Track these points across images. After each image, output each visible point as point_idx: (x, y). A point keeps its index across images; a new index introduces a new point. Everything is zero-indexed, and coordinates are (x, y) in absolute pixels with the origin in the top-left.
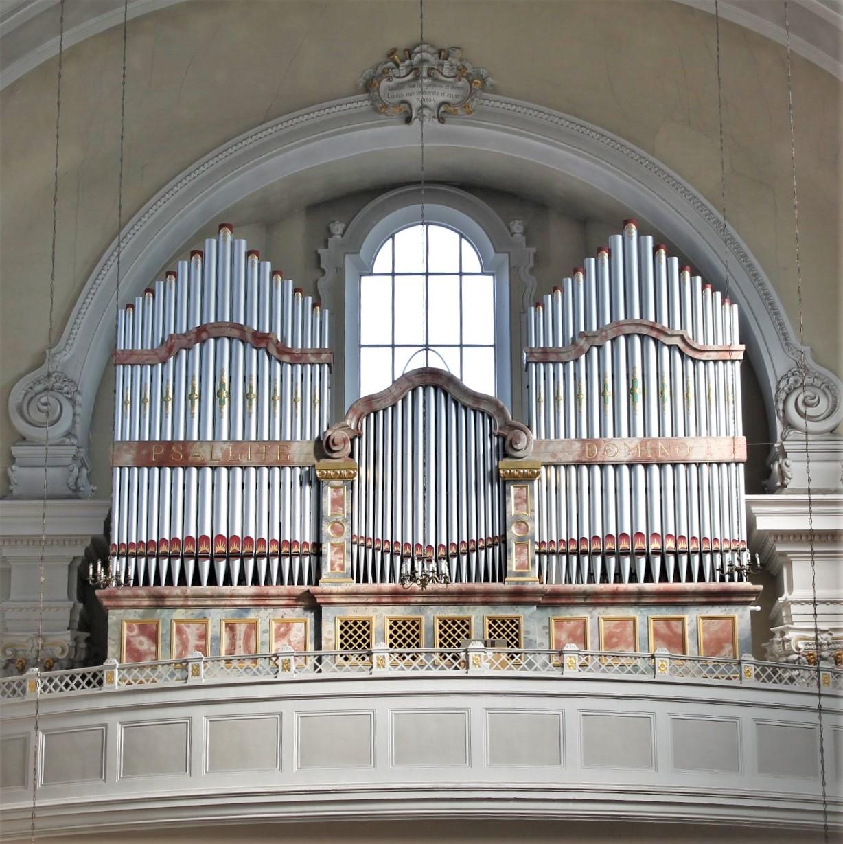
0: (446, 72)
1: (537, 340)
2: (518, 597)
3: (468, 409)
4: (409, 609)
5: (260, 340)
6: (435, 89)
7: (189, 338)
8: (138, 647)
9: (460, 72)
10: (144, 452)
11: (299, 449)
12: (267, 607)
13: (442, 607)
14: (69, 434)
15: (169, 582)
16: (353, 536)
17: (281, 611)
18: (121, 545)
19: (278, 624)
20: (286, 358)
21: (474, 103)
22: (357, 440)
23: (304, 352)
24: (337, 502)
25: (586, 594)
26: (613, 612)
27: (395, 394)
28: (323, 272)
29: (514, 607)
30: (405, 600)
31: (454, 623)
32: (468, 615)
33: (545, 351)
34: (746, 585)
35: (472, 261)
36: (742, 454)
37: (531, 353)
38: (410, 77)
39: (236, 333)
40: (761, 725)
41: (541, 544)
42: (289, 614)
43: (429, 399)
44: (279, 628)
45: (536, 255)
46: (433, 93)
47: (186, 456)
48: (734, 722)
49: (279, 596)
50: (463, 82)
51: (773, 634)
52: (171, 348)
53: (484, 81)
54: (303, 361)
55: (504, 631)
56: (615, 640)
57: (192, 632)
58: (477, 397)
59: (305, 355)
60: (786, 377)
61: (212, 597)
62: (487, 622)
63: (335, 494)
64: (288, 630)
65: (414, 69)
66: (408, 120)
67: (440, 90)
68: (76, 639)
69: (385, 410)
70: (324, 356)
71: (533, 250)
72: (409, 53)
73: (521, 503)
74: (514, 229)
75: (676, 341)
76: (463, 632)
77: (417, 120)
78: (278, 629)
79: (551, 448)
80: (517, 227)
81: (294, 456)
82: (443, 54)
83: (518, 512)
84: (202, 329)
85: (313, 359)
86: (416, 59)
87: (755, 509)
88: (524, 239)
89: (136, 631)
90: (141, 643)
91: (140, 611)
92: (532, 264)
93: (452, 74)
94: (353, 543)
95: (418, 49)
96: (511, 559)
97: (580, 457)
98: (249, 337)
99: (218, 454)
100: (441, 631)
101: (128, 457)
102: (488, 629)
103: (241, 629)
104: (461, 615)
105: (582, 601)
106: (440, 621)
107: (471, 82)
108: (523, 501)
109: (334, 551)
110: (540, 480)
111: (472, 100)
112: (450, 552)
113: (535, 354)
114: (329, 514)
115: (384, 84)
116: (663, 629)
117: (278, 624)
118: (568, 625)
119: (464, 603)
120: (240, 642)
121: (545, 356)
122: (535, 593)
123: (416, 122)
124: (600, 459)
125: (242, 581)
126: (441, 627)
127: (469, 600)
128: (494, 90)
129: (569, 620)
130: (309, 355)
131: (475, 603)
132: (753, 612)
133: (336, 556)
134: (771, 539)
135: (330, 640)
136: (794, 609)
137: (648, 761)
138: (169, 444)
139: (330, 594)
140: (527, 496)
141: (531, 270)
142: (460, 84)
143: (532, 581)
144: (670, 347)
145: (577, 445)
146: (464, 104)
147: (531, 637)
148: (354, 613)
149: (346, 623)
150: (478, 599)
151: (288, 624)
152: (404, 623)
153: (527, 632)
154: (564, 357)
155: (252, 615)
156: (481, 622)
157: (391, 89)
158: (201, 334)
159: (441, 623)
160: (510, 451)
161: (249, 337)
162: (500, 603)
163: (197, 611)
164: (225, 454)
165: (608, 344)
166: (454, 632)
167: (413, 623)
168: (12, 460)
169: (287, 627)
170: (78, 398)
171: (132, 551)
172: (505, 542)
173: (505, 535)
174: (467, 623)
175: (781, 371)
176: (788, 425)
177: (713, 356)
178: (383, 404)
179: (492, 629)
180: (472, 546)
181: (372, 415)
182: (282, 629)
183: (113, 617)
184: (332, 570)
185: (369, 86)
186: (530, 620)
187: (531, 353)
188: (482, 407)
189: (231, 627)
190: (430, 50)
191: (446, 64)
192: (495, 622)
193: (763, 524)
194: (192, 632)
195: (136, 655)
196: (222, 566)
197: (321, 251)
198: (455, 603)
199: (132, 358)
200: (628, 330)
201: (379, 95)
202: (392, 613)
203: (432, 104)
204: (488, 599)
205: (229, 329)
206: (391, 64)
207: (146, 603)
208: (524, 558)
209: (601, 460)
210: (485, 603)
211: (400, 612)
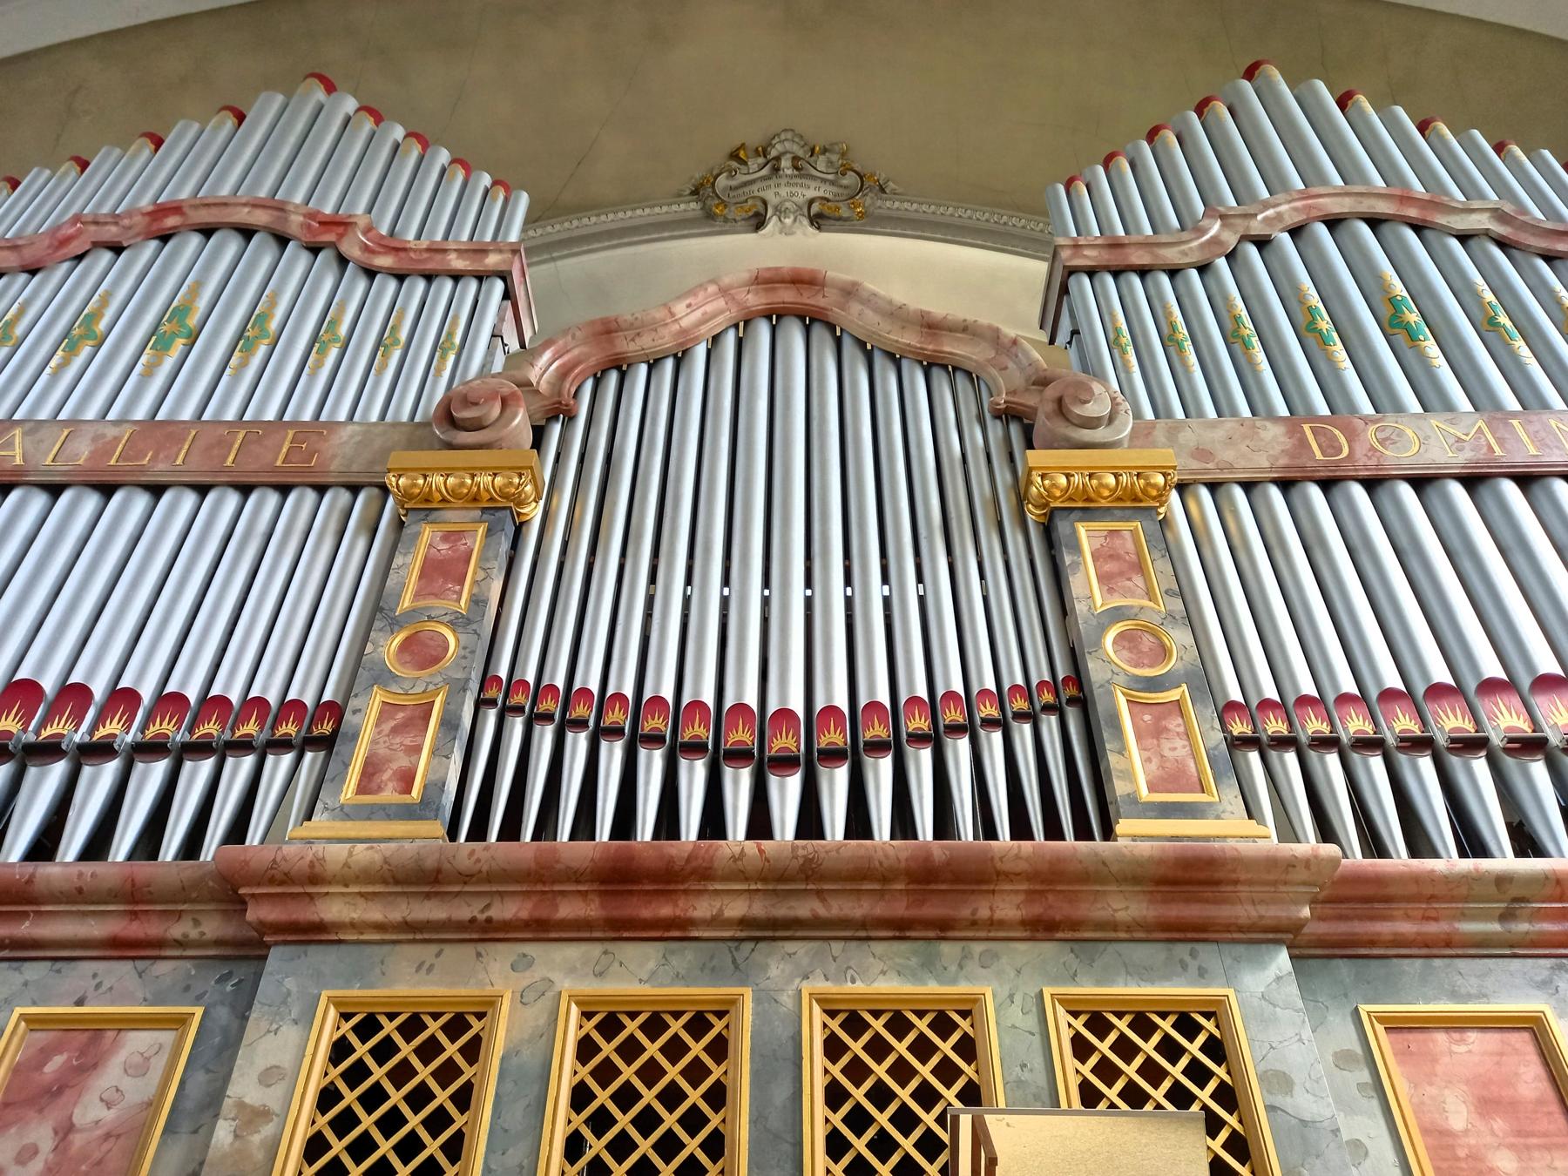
0: (821, 165)
3: (905, 364)
4: (686, 956)
6: (804, 181)
7: (126, 222)
11: (358, 438)
13: (837, 947)
16: (487, 679)
19: (42, 1038)
21: (868, 201)
22: (556, 429)
27: (685, 323)
29: (1182, 950)
30: (665, 911)
31: (899, 1025)
32: (963, 988)
38: (765, 172)
44: (45, 1054)
49: (78, 897)
54: (430, 266)
55: (1153, 1073)
59: (438, 257)
62: (1064, 1027)
63: (444, 546)
64: (87, 1064)
67: (813, 184)
69: (654, 365)
73: (1121, 574)
76: (947, 1072)
77: (774, 218)
81: (334, 456)
83: (1118, 601)
85: (458, 263)
93: (831, 170)
94: (480, 704)
95: (777, 140)
96: (1122, 750)
97: (1293, 457)
99: (82, 452)
100: (836, 1070)
102: (1072, 1062)
104: (932, 988)
106: (832, 1014)
107: (861, 178)
109: (387, 727)
111: (866, 195)
112: (867, 735)
113: (1087, 252)
114: (406, 602)
117: (42, 1038)
118: (1462, 1049)
119: (943, 929)
124: (1365, 464)
126: (833, 1048)
127: (965, 913)
129: (1457, 1025)
130: (453, 256)
131: (993, 929)
133: (398, 740)
135: (263, 1114)
139: (314, 878)
140: (1139, 553)
142: (845, 182)
144: (1464, 238)
145: (1273, 433)
147: (1303, 1103)
149: (367, 1027)
152: (654, 1026)
153: (1280, 1081)
154: (1172, 256)
156: (1031, 1022)
159: (835, 1025)
162: (1110, 932)
166: (902, 1072)
167: (698, 1026)
169: (82, 1053)
172: (1083, 703)
173: (1078, 676)
174: (964, 1024)
179: (1093, 1060)
181: (613, 377)
182: (56, 1062)
184: (362, 789)
190: (797, 140)
191: (822, 158)
192: (1099, 1025)
198: (900, 929)
201: (714, 191)
202: (600, 975)
203: (800, 200)
205: (246, 210)
208: (1176, 748)
209: (1373, 462)
210: (1041, 928)
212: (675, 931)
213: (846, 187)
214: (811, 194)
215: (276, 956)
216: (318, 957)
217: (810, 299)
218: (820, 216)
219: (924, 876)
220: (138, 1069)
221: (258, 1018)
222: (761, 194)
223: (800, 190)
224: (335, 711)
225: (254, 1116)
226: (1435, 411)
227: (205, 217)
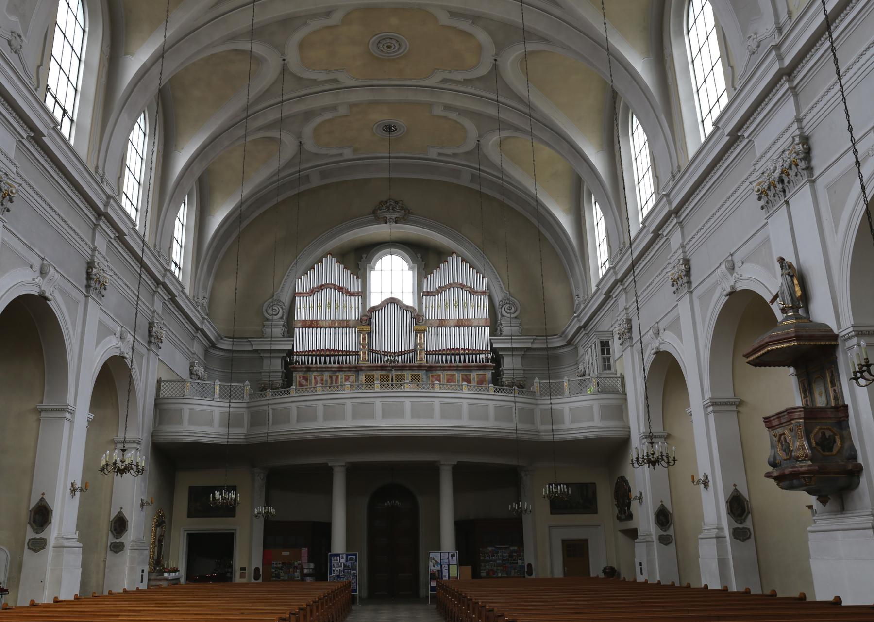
1: (426, 288)
2: (420, 367)
4: (386, 372)
5: (340, 289)
6: (394, 213)
8: (303, 383)
9: (402, 208)
10: (304, 323)
12: (342, 371)
14: (281, 318)
15: (312, 363)
16: (369, 349)
17: (347, 372)
18: (297, 352)
20: (348, 294)
23: (354, 293)
24: (364, 339)
25: (441, 367)
26: (449, 373)
28: (360, 269)
33: (428, 292)
34: (490, 364)
35: (405, 265)
36: (489, 324)
37: (424, 293)
39: (333, 286)
40: (496, 406)
41: (427, 351)
42: (349, 373)
43: (392, 307)
45: (425, 264)
46: (394, 215)
47: (317, 324)
48: (487, 405)
49: (346, 368)
50: (403, 211)
51: (498, 380)
52: (312, 292)
53: (409, 211)
56: (450, 381)
57: (319, 379)
58: (408, 307)
60: (502, 301)
61: (325, 368)
64: (349, 378)
65: (388, 208)
66: (386, 223)
67: (396, 214)
68: (283, 381)
69: (379, 310)
70: (360, 294)
71: (424, 263)
72: (386, 202)
74: (418, 256)
75: (468, 289)
78: (345, 378)
79: (430, 322)
80: (419, 256)
82: (396, 202)
84: (322, 285)
86: (388, 204)
87: (492, 341)
88: (421, 259)
89: (302, 379)
90: (303, 382)
91: (303, 372)
92: (424, 267)
94: (369, 351)
98: (337, 287)
99: (327, 324)
101: (299, 325)
103: (334, 378)
105: (439, 369)
107: (405, 211)
108: (421, 338)
110: (427, 332)
115: (379, 211)
116: (464, 377)
120: (334, 382)
121: (428, 294)
122: (425, 366)
123: (388, 223)
125: (334, 363)
128: (412, 214)
129: (436, 375)
131: (407, 370)
132: (492, 372)
134: (498, 350)
136: (504, 372)
137: (487, 418)
138: (312, 320)
139: (362, 367)
141: (424, 269)
143: (424, 363)
144: (466, 291)
146: (403, 218)
148: (369, 373)
150: (407, 369)
151: (349, 376)
154: (434, 294)
155: (337, 374)
157: (381, 213)
158: (322, 287)
160: (417, 323)
161: (337, 287)
163: (321, 372)
164: (329, 324)
165: (448, 290)
168: (264, 326)
170: (284, 307)
171: (300, 354)
175: (500, 299)
176: (502, 316)
177: (480, 293)
178: (378, 308)
180: (406, 352)
183: (294, 375)
185: (374, 212)
186: (422, 374)
187: (424, 293)
188: (409, 309)
189: (331, 377)
193: (495, 346)
194: (319, 379)
195: (301, 385)
196: (328, 359)
197: (359, 263)
198: (400, 370)
199: (301, 294)
200: (453, 286)
204: (411, 368)
206: (381, 206)
207: (305, 370)
210: (409, 370)
211: (383, 373)
212: (386, 370)
213: (402, 213)
214: (395, 216)
215: (360, 372)
216: (363, 372)
217: (394, 301)
218: (397, 220)
219: (402, 367)
220: (352, 378)
221: (360, 376)
222: (386, 216)
223: (393, 216)
224: (358, 352)
225: (361, 381)
226: (577, 173)
227: (326, 286)
